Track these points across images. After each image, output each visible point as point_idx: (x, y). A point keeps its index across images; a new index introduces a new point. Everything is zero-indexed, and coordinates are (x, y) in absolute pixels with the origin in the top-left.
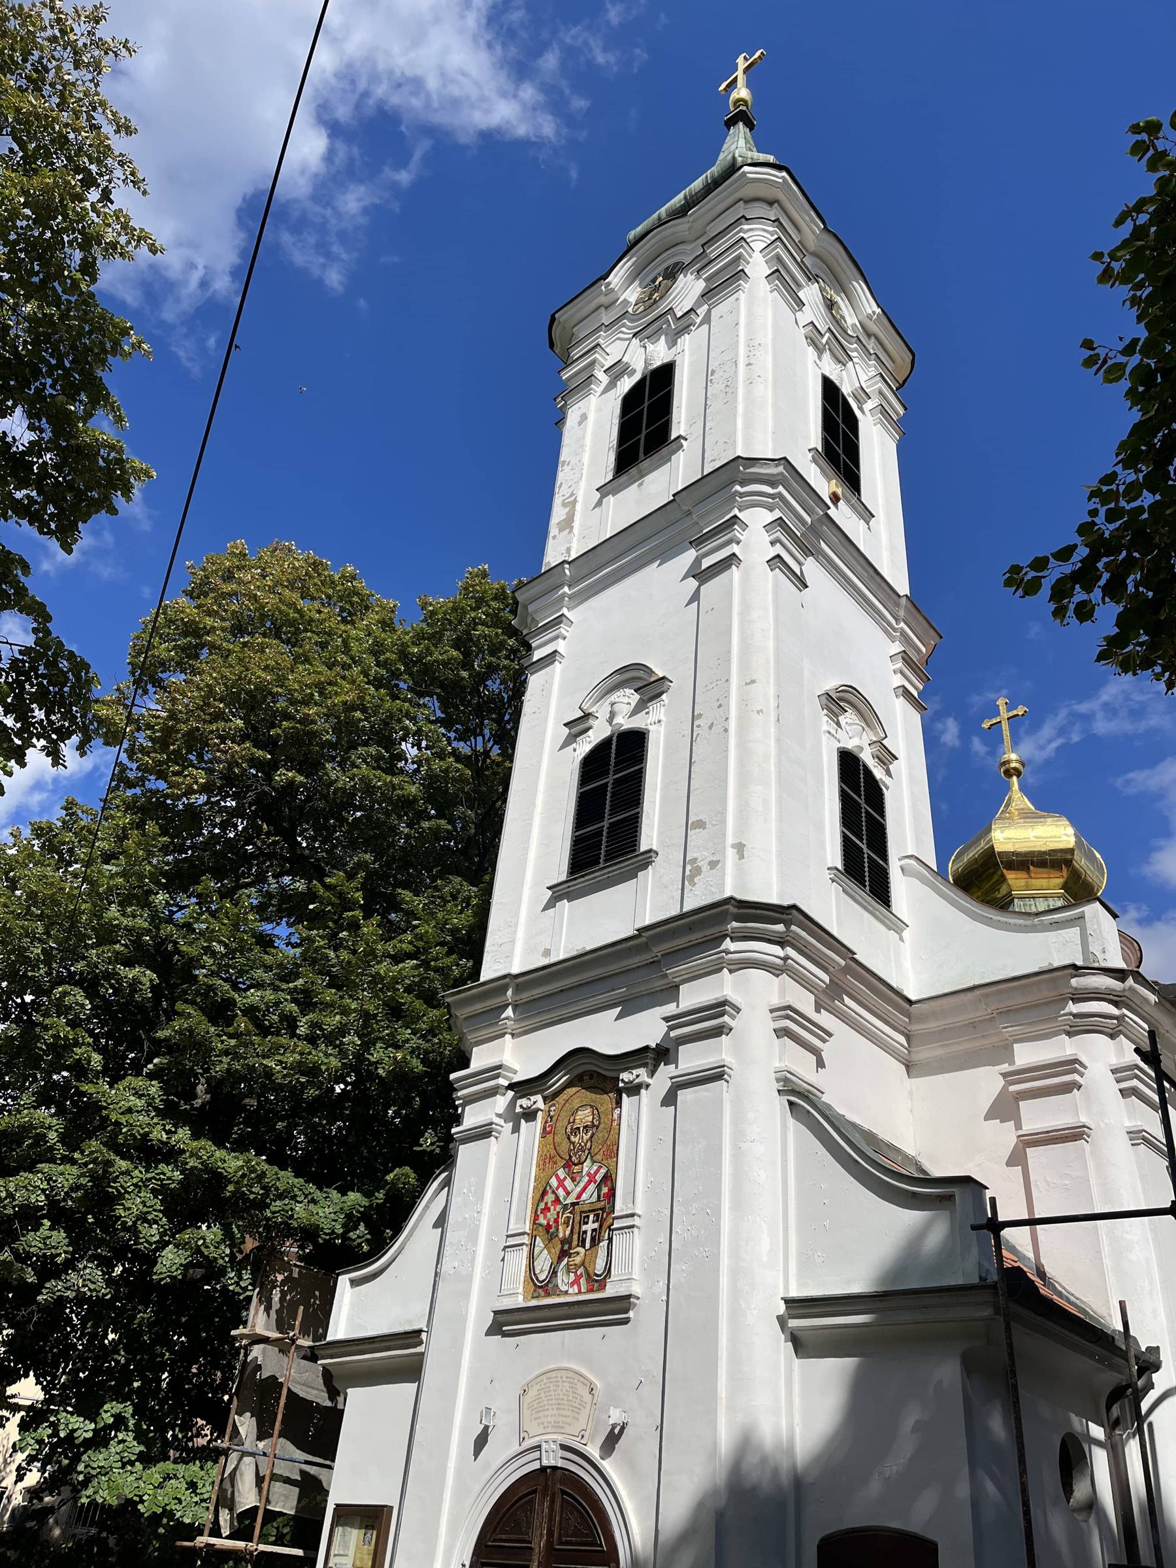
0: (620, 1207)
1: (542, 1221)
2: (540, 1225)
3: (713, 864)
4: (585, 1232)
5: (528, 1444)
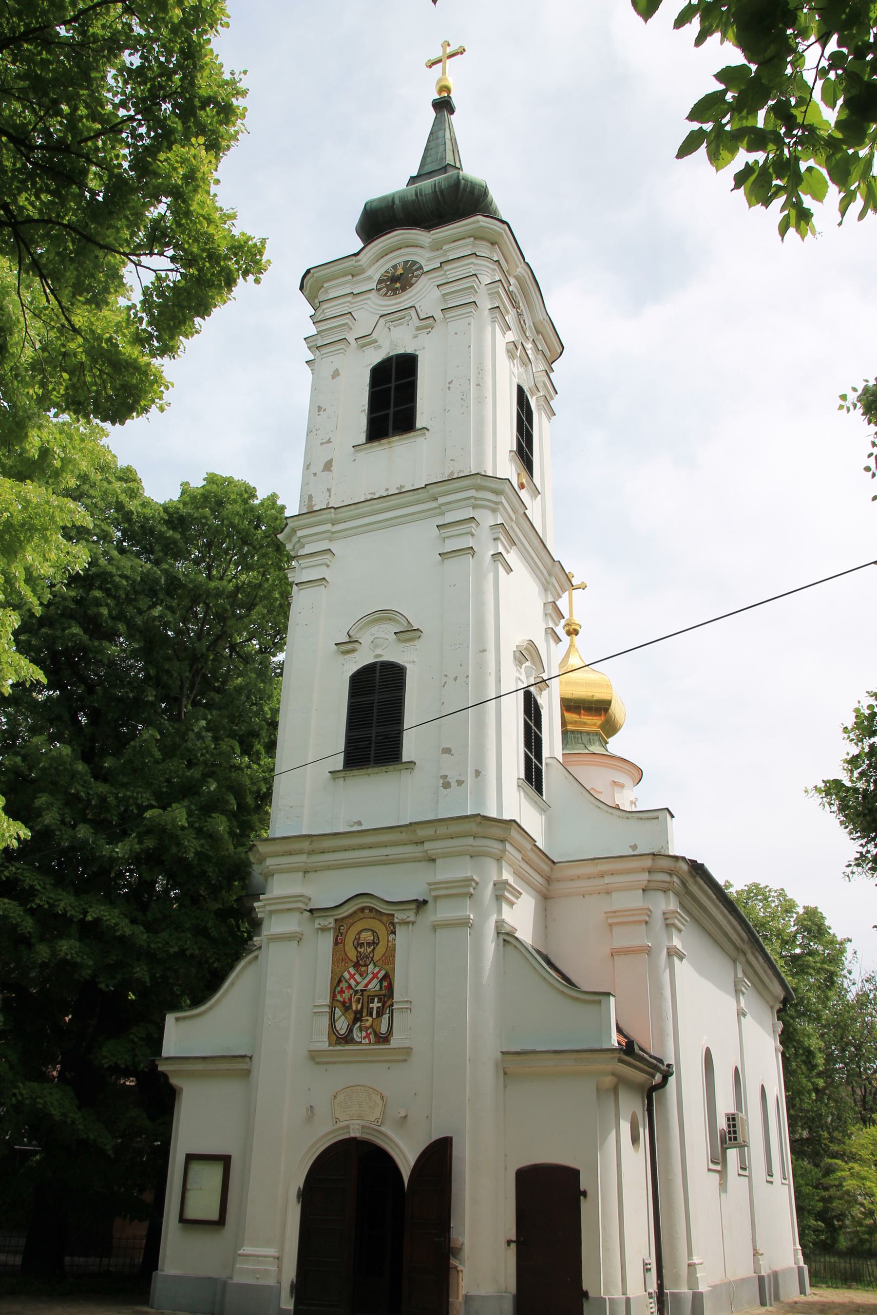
0: (397, 997)
1: (339, 997)
3: (460, 783)
4: (372, 1008)
5: (340, 1125)
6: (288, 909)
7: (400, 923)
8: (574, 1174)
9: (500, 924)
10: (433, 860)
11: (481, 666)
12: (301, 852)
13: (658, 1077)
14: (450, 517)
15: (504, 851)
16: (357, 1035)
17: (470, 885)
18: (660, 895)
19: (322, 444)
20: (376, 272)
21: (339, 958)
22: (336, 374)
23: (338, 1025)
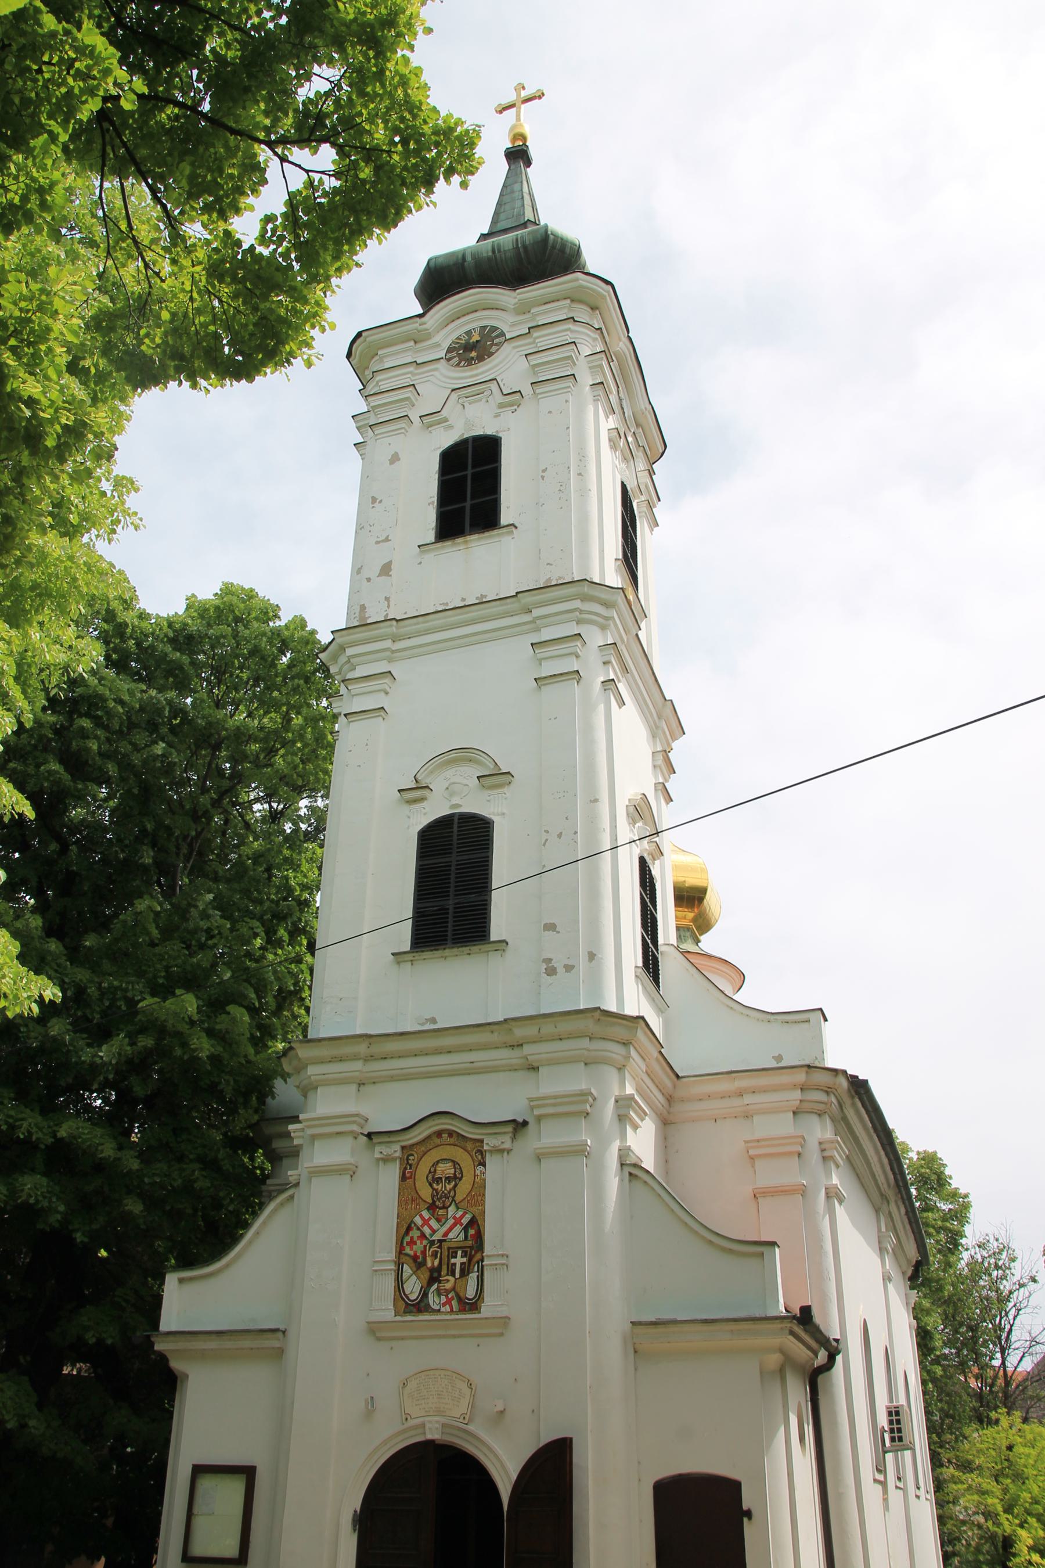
0: (488, 1249)
1: (408, 1250)
2: (407, 1255)
3: (569, 968)
4: (455, 1264)
5: (411, 1423)
6: (337, 1133)
7: (491, 1151)
8: (733, 1488)
9: (624, 1152)
10: (534, 1069)
11: (592, 819)
12: (355, 1058)
13: (822, 1356)
14: (546, 634)
15: (628, 1057)
16: (433, 1300)
17: (587, 1101)
18: (815, 1119)
19: (377, 543)
20: (446, 338)
21: (407, 1196)
22: (395, 458)
23: (408, 1287)
